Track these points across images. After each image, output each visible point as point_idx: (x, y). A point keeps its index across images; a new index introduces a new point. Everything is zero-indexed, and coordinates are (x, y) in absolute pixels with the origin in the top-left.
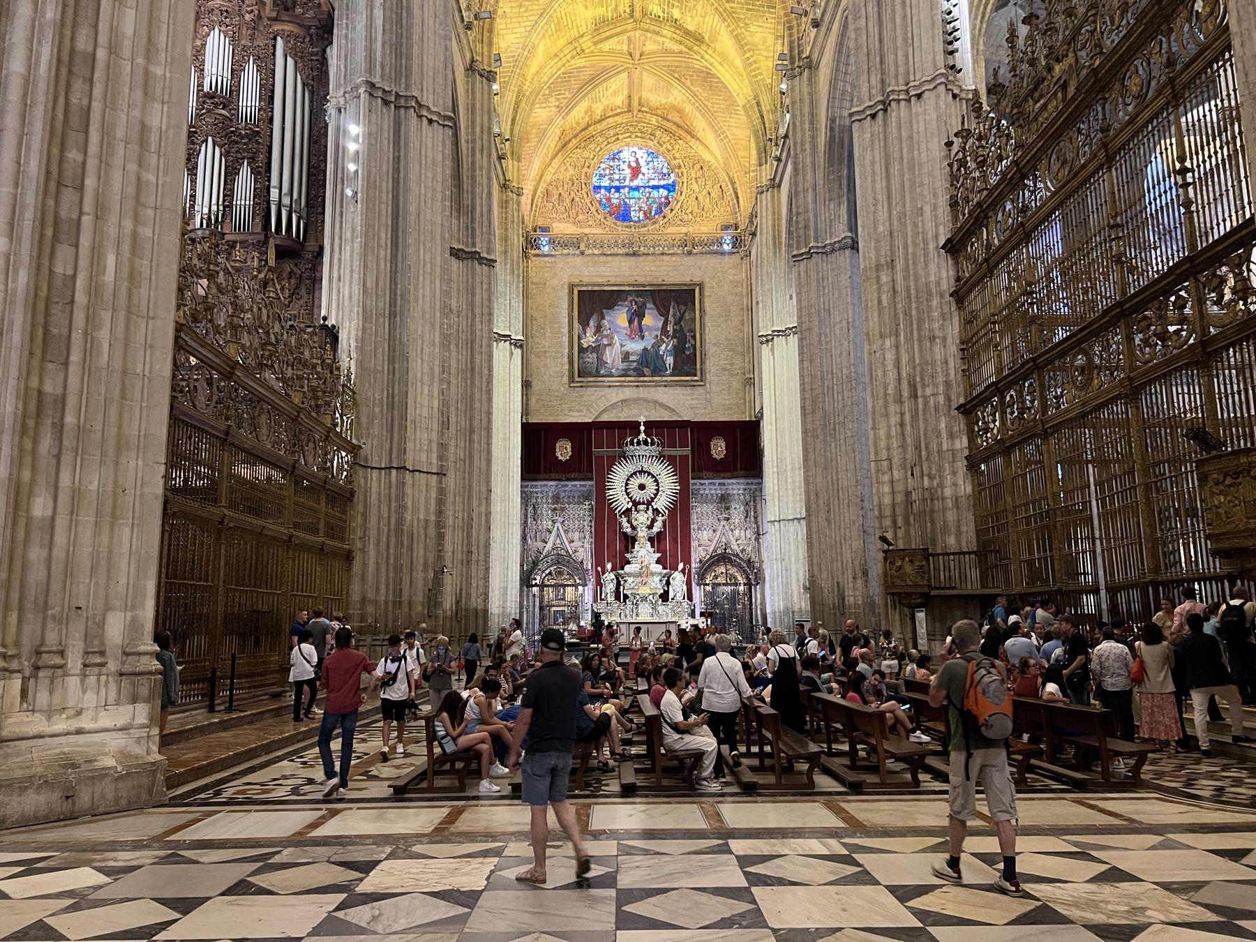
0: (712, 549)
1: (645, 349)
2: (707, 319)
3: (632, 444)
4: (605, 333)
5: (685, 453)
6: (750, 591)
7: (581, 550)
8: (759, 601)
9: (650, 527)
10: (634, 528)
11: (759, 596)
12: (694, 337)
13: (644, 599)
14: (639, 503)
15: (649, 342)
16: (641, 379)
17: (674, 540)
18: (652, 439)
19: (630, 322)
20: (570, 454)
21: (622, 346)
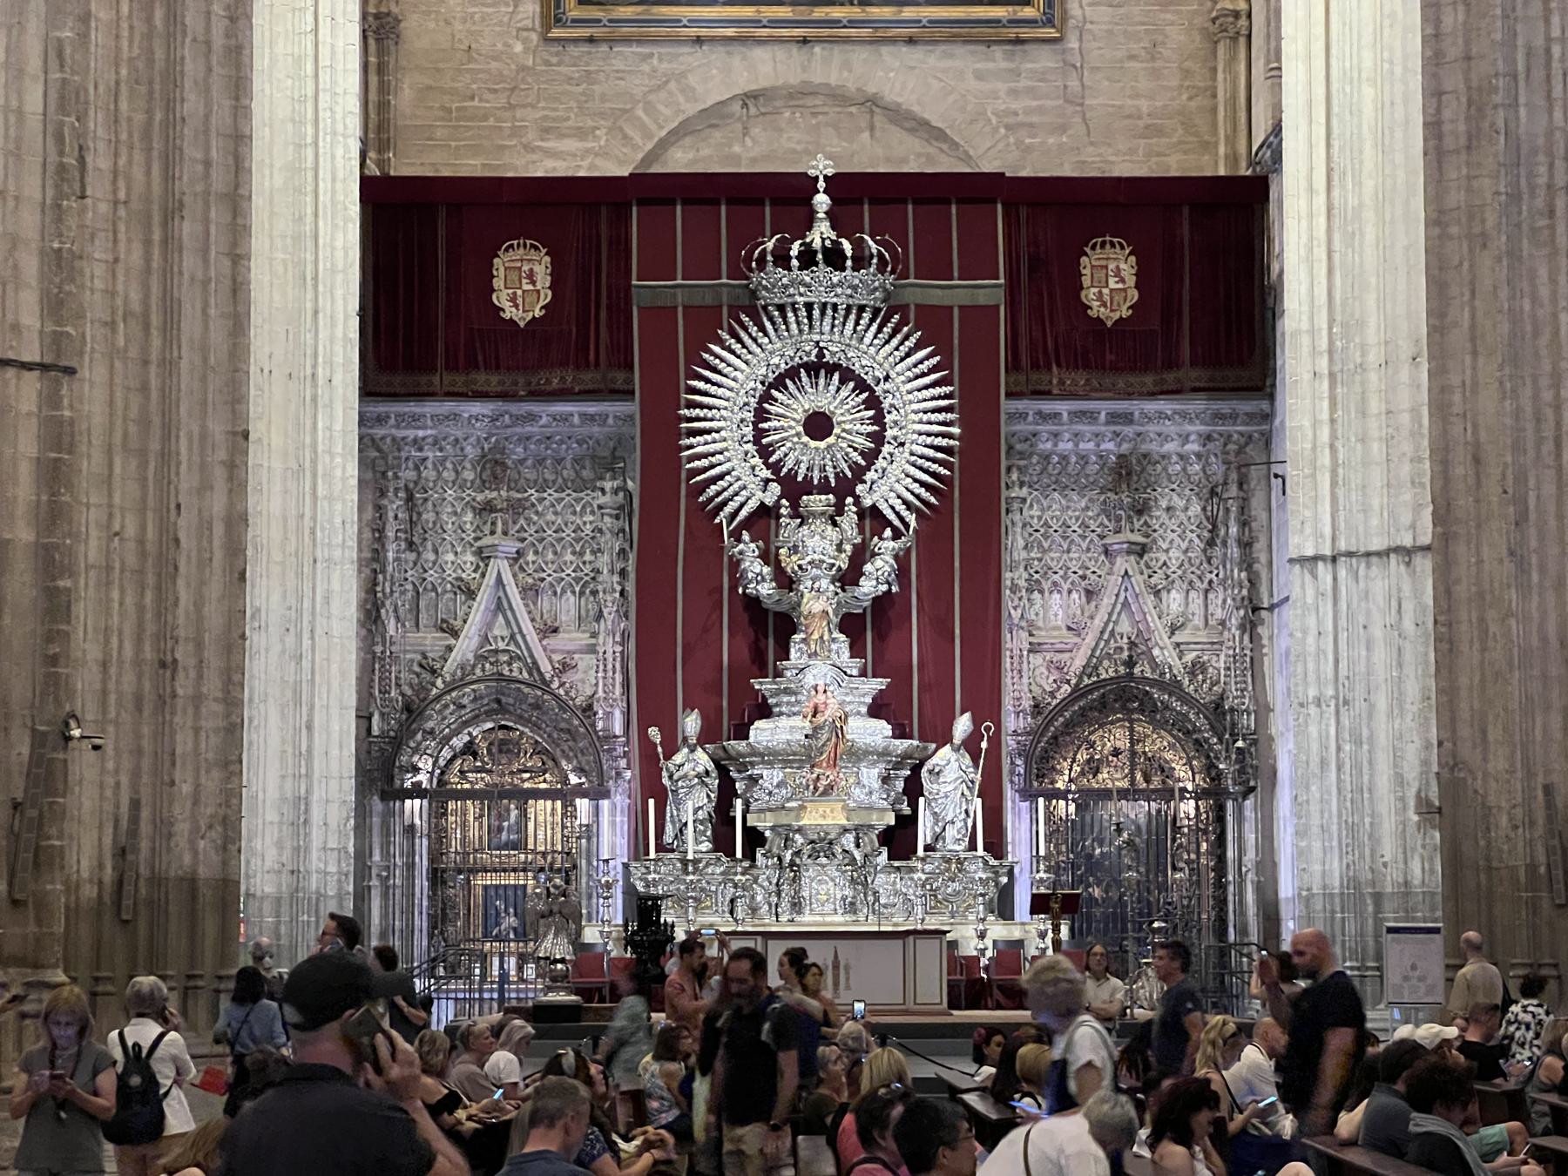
0: (1079, 662)
3: (782, 260)
5: (983, 298)
6: (1220, 819)
7: (585, 661)
8: (1250, 856)
9: (849, 577)
10: (786, 582)
11: (1250, 838)
13: (823, 846)
14: (808, 488)
17: (939, 627)
18: (858, 245)
20: (547, 297)
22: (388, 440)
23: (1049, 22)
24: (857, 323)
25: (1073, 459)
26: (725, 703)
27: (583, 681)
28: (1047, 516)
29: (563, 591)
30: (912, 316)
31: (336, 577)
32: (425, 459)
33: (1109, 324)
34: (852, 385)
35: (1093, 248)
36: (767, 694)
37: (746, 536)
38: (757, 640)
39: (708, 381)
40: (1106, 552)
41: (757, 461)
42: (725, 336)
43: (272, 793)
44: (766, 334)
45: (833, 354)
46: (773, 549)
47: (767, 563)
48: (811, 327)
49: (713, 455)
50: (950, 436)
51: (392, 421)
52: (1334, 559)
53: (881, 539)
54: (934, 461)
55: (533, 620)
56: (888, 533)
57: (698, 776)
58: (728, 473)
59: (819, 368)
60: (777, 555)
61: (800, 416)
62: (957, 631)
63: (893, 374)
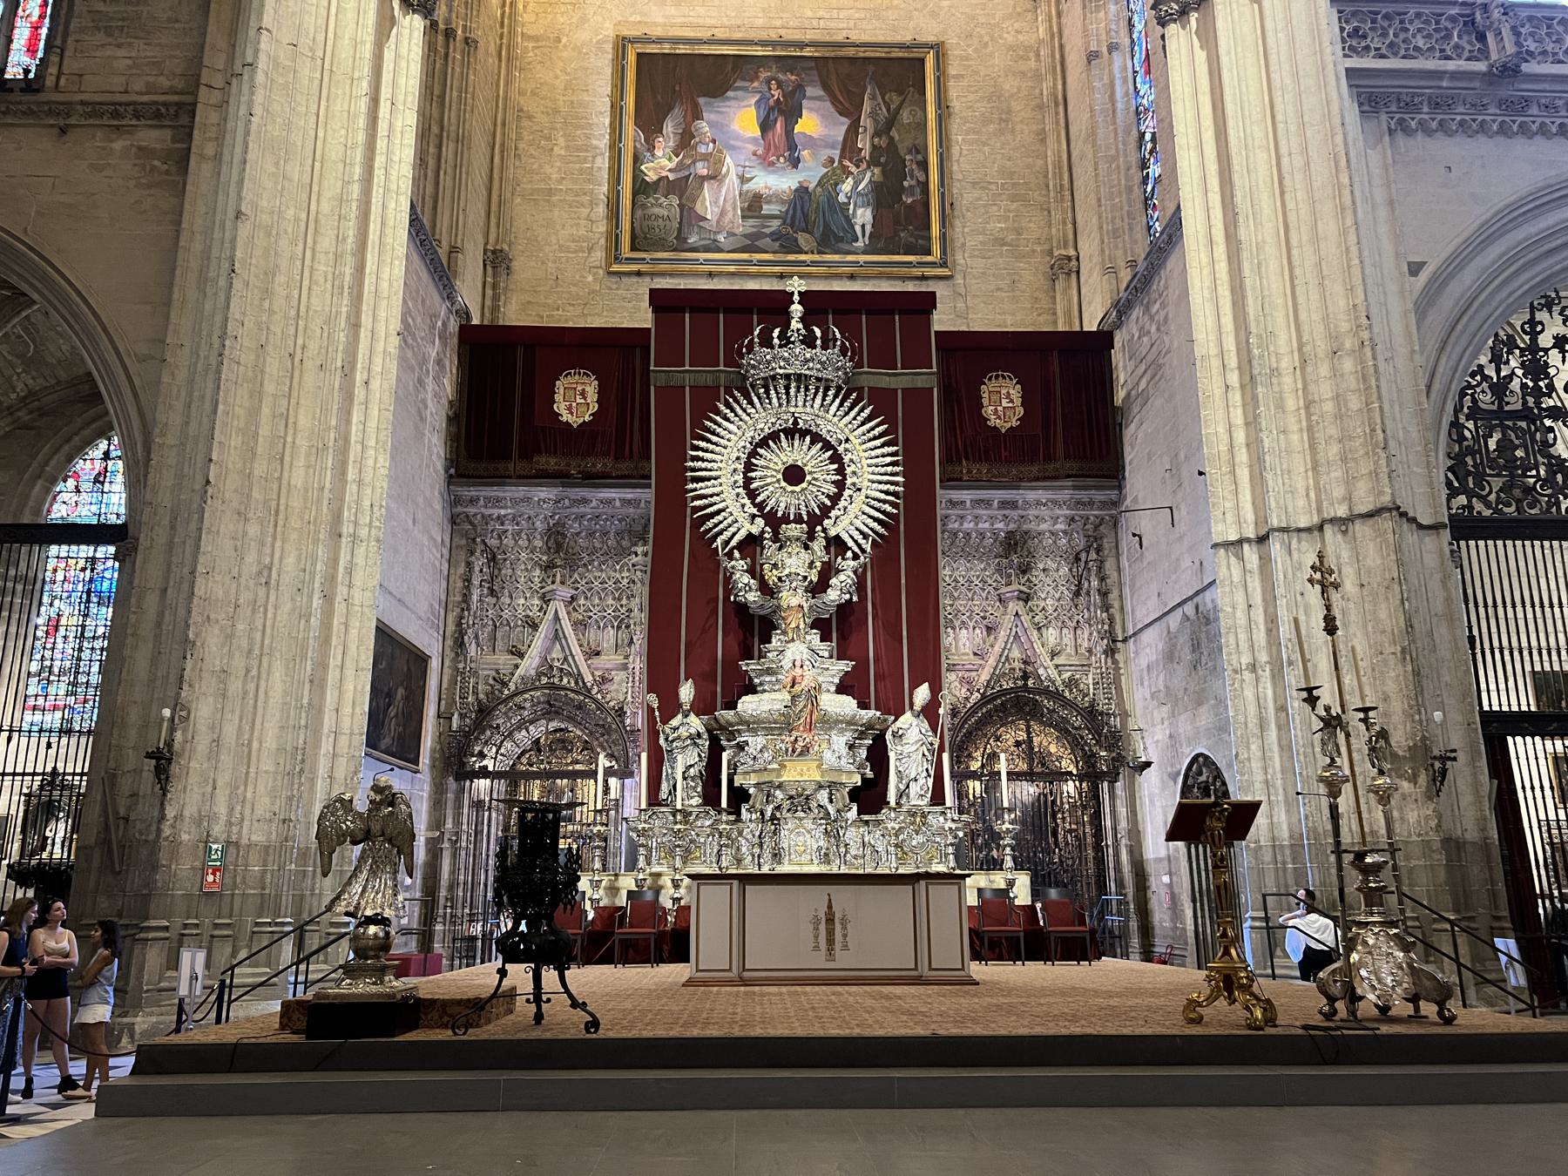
0: (985, 676)
1: (802, 191)
2: (954, 126)
3: (766, 342)
4: (702, 149)
5: (921, 382)
6: (1096, 797)
7: (619, 676)
8: (1123, 825)
9: (818, 587)
10: (767, 590)
11: (1122, 811)
12: (924, 165)
13: (800, 801)
14: (786, 519)
15: (811, 172)
16: (791, 257)
17: (890, 629)
19: (765, 126)
20: (594, 407)
21: (743, 180)
22: (479, 517)
23: (944, 265)
24: (824, 400)
25: (974, 535)
26: (719, 689)
27: (617, 691)
28: (956, 574)
29: (605, 626)
30: (866, 395)
31: (361, 551)
32: (506, 531)
33: (1003, 431)
34: (820, 445)
35: (990, 379)
36: (752, 674)
37: (737, 554)
38: (745, 638)
39: (709, 441)
40: (1000, 600)
41: (746, 501)
42: (722, 407)
43: (270, 742)
44: (754, 407)
45: (806, 421)
46: (758, 567)
47: (753, 578)
48: (788, 402)
49: (711, 496)
50: (896, 484)
51: (482, 503)
52: (1262, 540)
53: (843, 559)
54: (884, 502)
55: (581, 646)
56: (849, 554)
57: (690, 737)
58: (723, 510)
59: (793, 432)
60: (762, 570)
61: (781, 467)
62: (905, 633)
63: (851, 438)
